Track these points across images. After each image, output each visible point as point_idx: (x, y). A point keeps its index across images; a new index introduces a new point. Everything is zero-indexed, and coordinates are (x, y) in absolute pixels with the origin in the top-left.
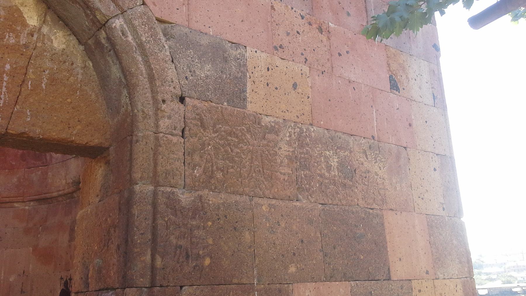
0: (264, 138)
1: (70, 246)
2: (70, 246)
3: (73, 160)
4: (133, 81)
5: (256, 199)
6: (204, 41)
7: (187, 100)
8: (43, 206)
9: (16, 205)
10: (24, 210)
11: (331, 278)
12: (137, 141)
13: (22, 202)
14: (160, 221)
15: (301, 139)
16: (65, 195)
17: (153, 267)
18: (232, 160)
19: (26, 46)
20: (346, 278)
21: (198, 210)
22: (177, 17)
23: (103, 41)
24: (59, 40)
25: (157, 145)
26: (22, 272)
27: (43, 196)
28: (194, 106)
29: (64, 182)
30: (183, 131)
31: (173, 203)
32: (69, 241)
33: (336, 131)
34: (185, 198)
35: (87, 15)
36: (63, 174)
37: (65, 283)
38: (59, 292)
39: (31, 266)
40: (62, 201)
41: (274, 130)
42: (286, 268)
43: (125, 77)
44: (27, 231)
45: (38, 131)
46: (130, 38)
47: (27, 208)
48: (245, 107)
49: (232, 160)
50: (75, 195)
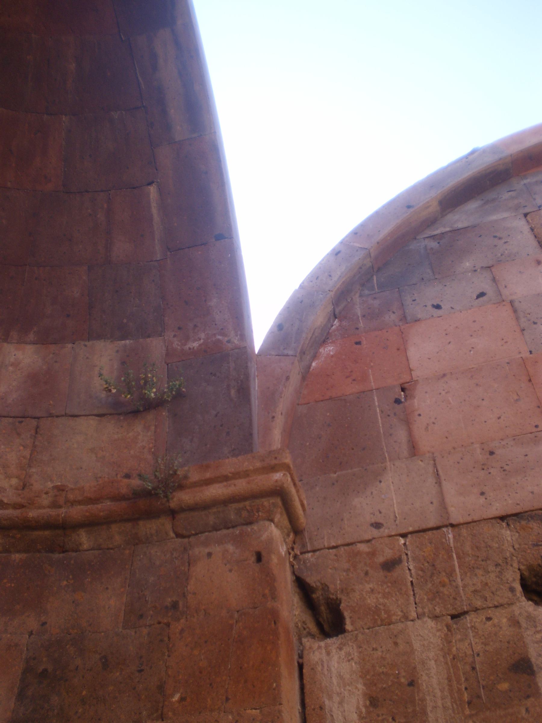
50: (84, 539)
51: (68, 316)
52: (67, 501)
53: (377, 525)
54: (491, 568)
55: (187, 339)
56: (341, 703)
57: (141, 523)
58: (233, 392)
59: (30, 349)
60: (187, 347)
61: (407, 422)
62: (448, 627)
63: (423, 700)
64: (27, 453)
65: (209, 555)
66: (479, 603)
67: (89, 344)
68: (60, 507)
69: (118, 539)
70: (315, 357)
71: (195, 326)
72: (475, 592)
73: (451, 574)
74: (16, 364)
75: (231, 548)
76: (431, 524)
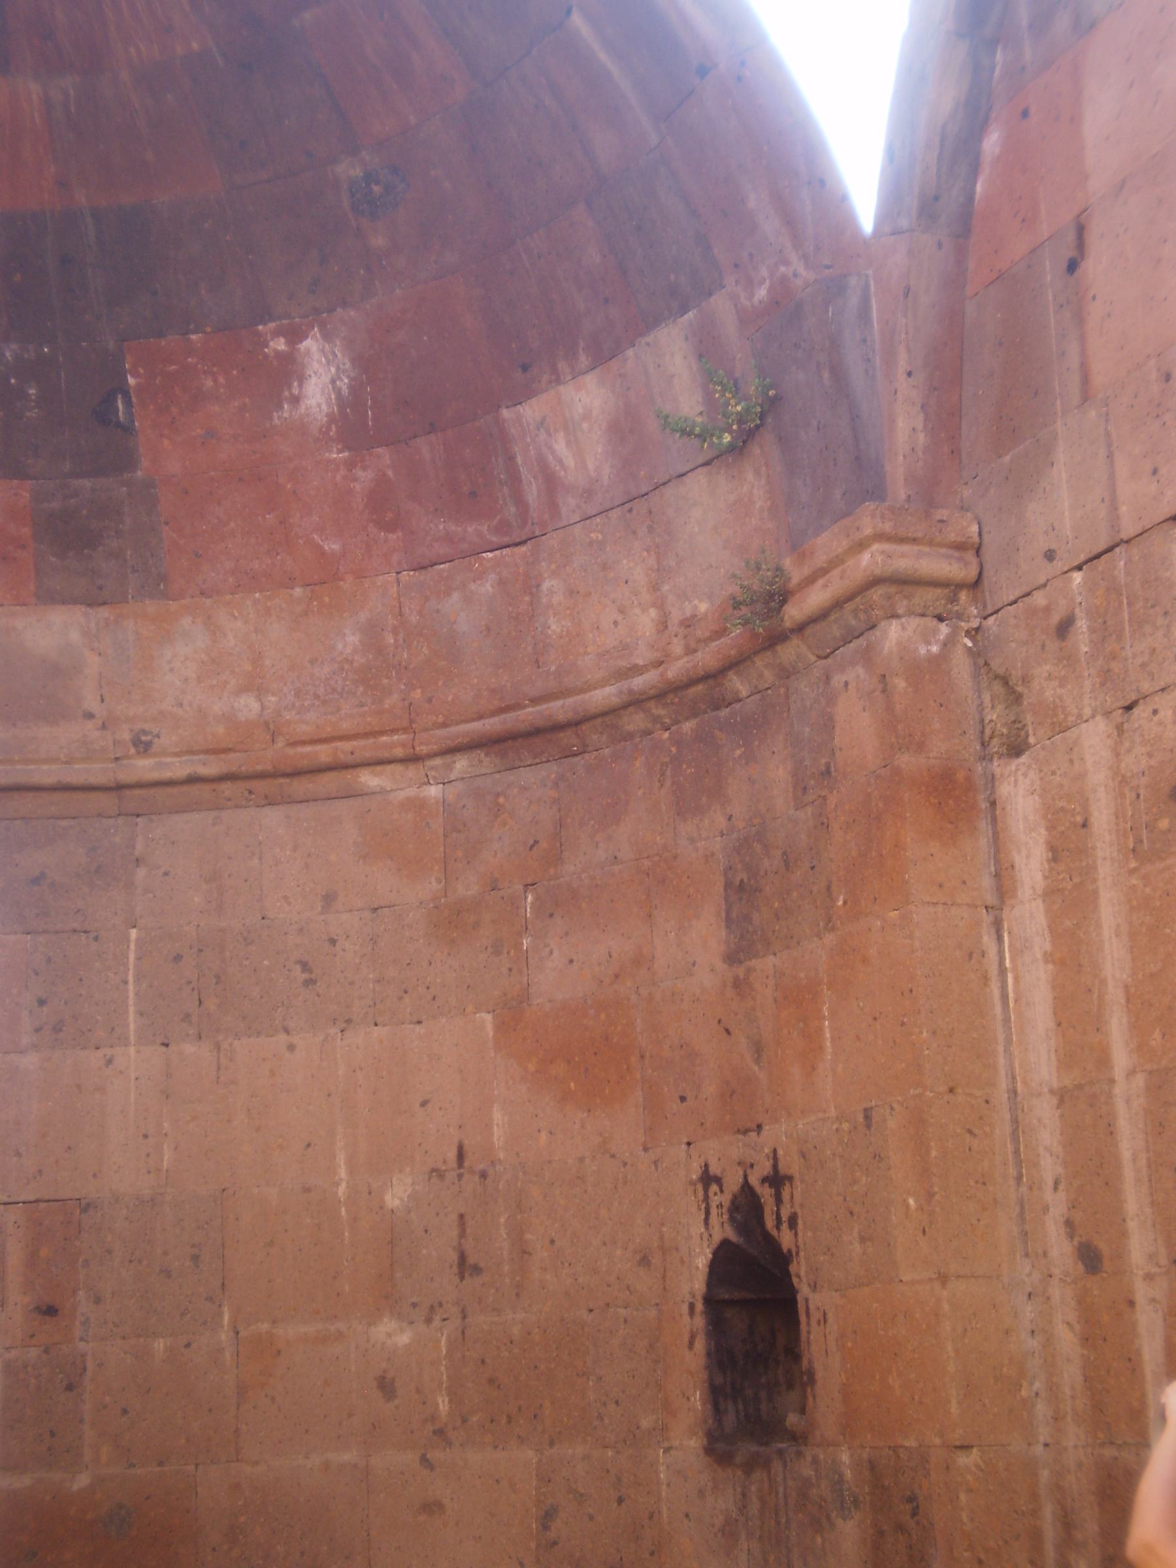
1: (740, 986)
2: (740, 986)
3: (697, 483)
8: (527, 776)
9: (369, 779)
10: (419, 806)
13: (404, 761)
16: (665, 693)
26: (452, 1155)
27: (529, 715)
29: (646, 621)
32: (732, 958)
36: (639, 575)
37: (735, 1207)
38: (702, 1261)
39: (497, 1115)
40: (648, 733)
44: (452, 921)
47: (434, 791)
50: (737, 684)
51: (606, 301)
52: (699, 641)
53: (1050, 556)
54: (1160, 621)
55: (750, 285)
56: (1028, 857)
57: (779, 648)
58: (826, 375)
59: (590, 380)
60: (756, 300)
61: (1080, 318)
62: (1120, 728)
63: (1094, 848)
64: (652, 561)
65: (846, 684)
66: (1146, 686)
67: (648, 339)
68: (695, 651)
69: (769, 675)
70: (975, 169)
71: (751, 255)
72: (1143, 665)
73: (1120, 638)
74: (587, 417)
75: (860, 670)
76: (1102, 546)
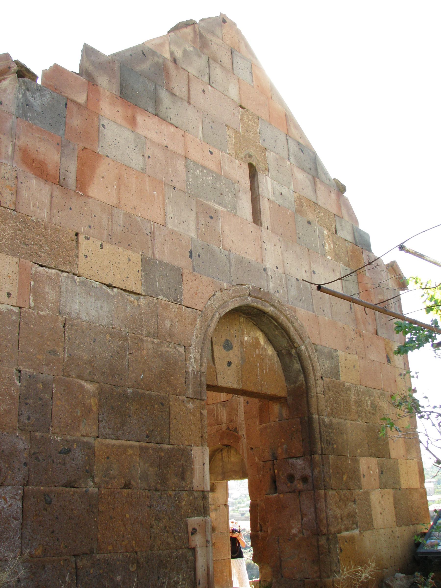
0: (346, 393)
4: (309, 372)
5: (346, 421)
6: (326, 350)
7: (324, 378)
11: (370, 456)
12: (312, 397)
14: (322, 430)
15: (358, 393)
17: (322, 447)
18: (338, 404)
19: (262, 355)
20: (375, 456)
21: (331, 425)
22: (317, 342)
23: (293, 353)
24: (270, 350)
25: (318, 399)
28: (326, 381)
30: (324, 392)
31: (324, 422)
33: (369, 387)
34: (327, 420)
35: (288, 343)
41: (349, 389)
42: (357, 450)
43: (303, 370)
45: (269, 391)
46: (307, 354)
48: (339, 379)
49: (338, 404)
